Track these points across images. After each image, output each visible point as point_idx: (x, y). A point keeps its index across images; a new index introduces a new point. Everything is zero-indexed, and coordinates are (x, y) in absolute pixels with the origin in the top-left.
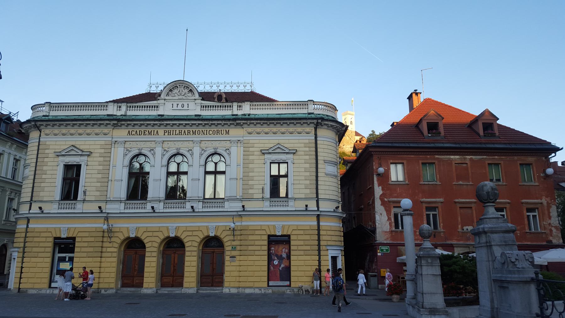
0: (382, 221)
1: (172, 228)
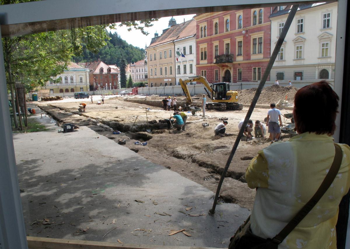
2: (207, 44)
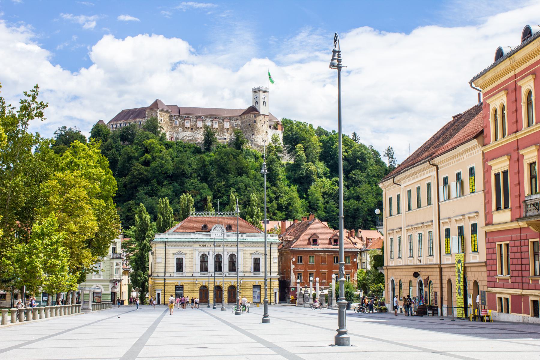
0: (293, 278)
1: (219, 282)
2: (510, 160)
